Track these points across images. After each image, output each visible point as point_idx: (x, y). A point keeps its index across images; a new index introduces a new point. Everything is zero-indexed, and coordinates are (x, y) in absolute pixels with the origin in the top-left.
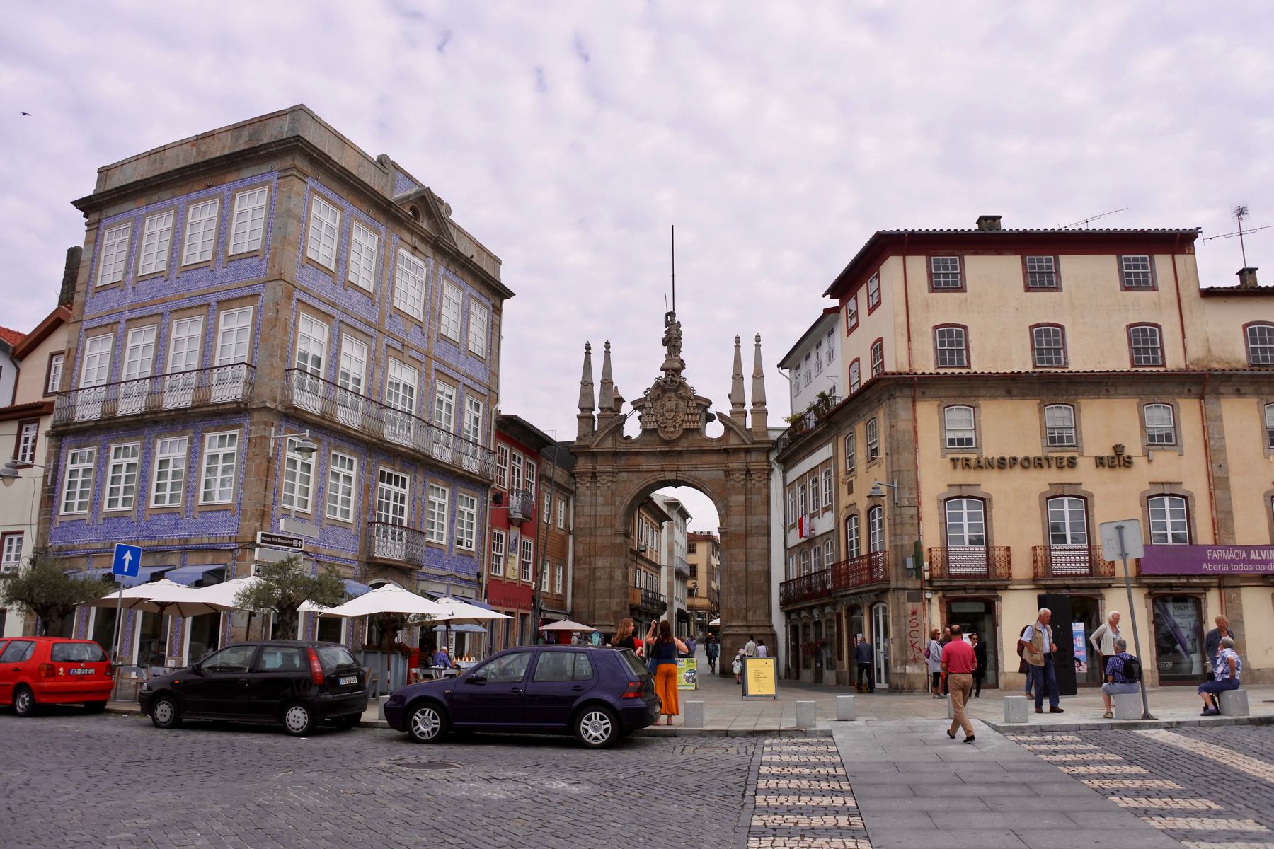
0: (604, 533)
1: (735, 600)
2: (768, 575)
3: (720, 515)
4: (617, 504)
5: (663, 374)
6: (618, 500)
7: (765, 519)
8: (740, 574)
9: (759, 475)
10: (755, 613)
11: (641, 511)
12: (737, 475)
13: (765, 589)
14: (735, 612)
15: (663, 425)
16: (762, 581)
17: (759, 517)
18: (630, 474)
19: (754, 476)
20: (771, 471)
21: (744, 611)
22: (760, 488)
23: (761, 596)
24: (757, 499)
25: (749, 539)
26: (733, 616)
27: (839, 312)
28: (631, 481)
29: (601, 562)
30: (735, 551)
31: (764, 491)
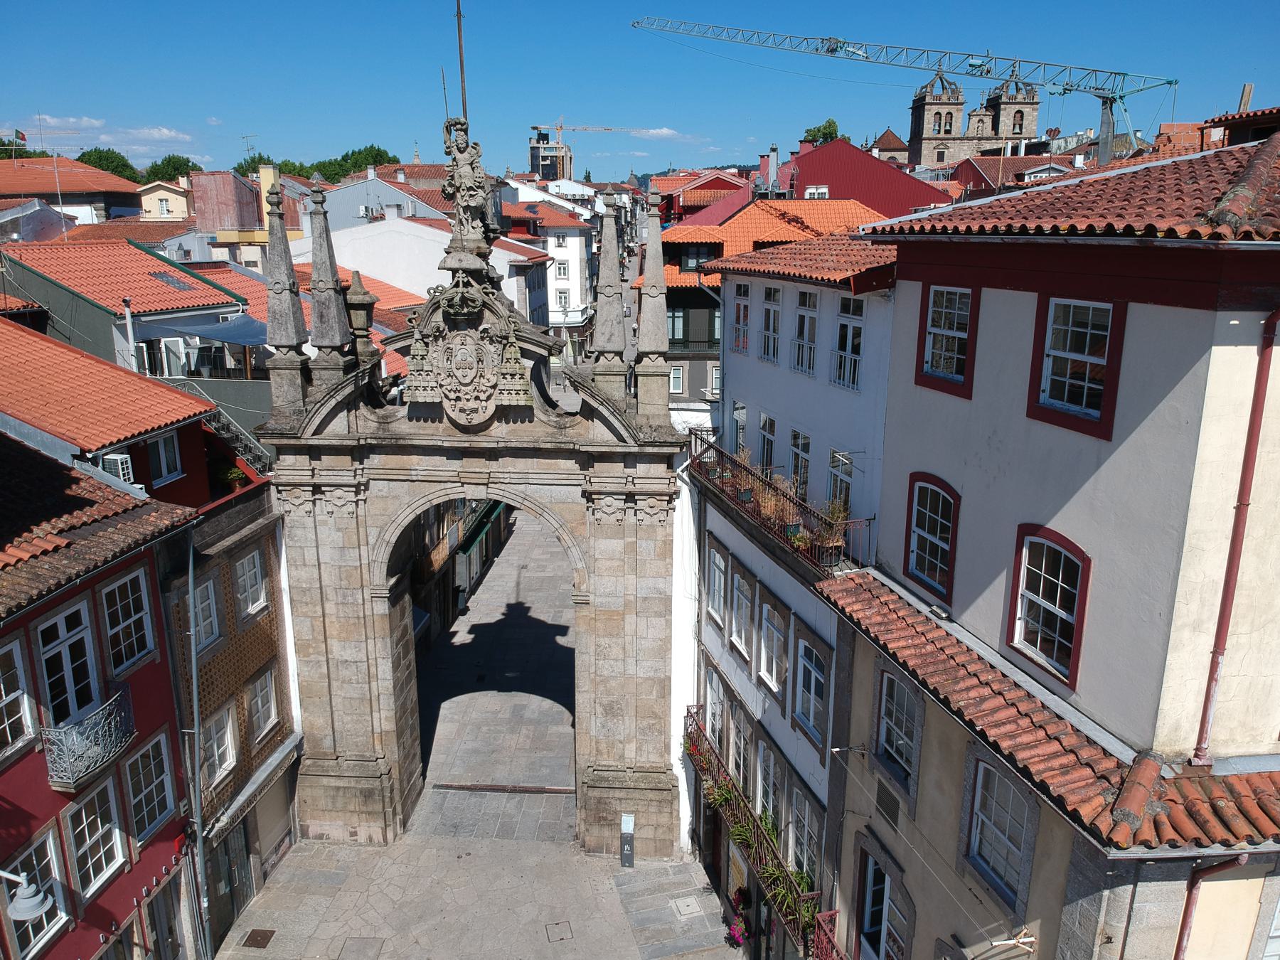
0: (350, 600)
1: (603, 727)
2: (664, 686)
4: (372, 540)
6: (373, 533)
8: (613, 684)
10: (639, 749)
12: (609, 500)
15: (452, 395)
16: (654, 696)
17: (651, 582)
24: (646, 547)
27: (892, 286)
28: (396, 497)
29: (349, 652)
30: (604, 642)
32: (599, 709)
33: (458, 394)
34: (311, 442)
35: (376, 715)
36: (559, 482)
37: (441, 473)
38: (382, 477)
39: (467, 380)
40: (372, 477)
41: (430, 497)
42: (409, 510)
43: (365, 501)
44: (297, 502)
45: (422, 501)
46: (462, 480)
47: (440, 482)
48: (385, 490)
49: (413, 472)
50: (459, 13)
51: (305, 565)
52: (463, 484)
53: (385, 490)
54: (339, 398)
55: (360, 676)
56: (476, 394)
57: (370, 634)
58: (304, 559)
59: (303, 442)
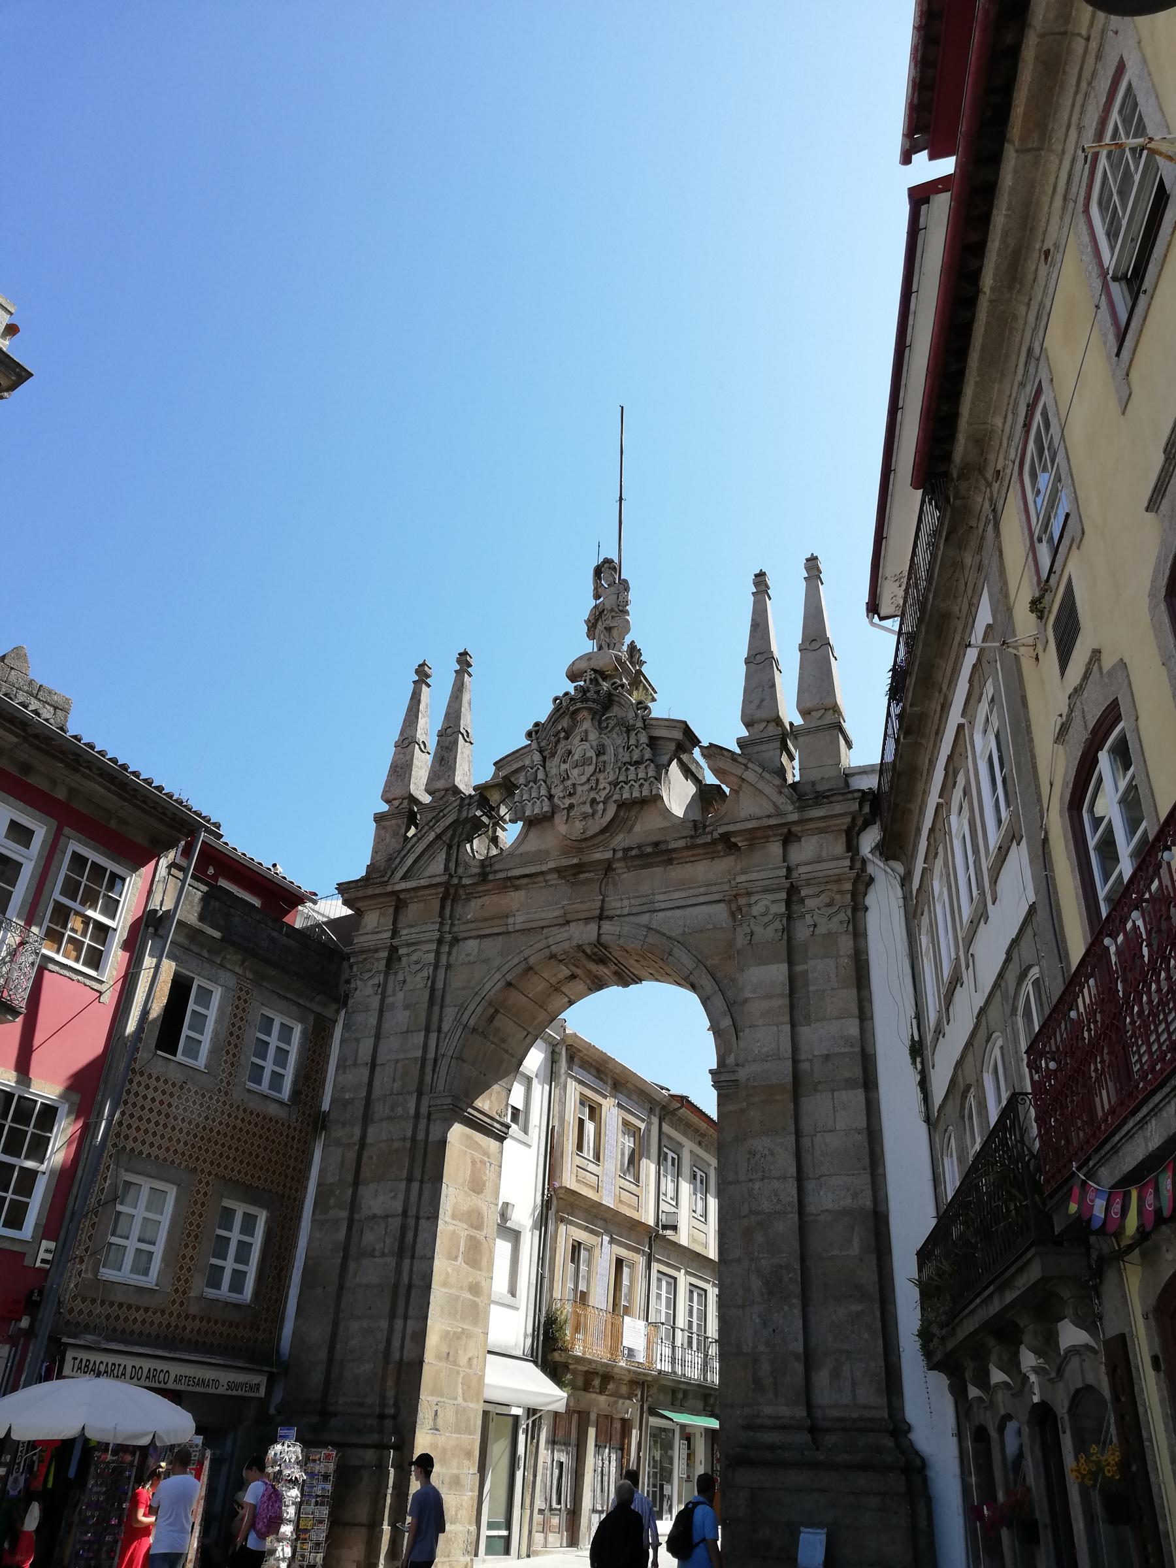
1: (765, 1323)
3: (715, 1029)
4: (446, 1027)
5: (570, 687)
6: (450, 1013)
7: (853, 1030)
9: (824, 898)
10: (836, 1374)
11: (666, 1128)
13: (868, 1277)
14: (765, 1367)
15: (567, 802)
16: (855, 1249)
18: (487, 942)
19: (810, 903)
20: (863, 882)
21: (799, 1367)
22: (830, 936)
23: (856, 1307)
25: (809, 1104)
26: (757, 1382)
28: (486, 961)
30: (761, 1144)
31: (846, 944)
32: (756, 1284)
33: (573, 801)
34: (398, 887)
35: (399, 1323)
36: (694, 900)
37: (544, 915)
38: (474, 933)
39: (584, 778)
40: (461, 935)
41: (527, 953)
42: (498, 976)
43: (449, 966)
44: (366, 976)
45: (516, 961)
46: (569, 917)
47: (543, 928)
48: (473, 954)
49: (511, 920)
50: (621, 499)
51: (355, 1065)
52: (568, 922)
53: (473, 954)
54: (438, 831)
55: (388, 1241)
56: (593, 794)
57: (417, 1174)
58: (356, 1058)
59: (389, 888)
